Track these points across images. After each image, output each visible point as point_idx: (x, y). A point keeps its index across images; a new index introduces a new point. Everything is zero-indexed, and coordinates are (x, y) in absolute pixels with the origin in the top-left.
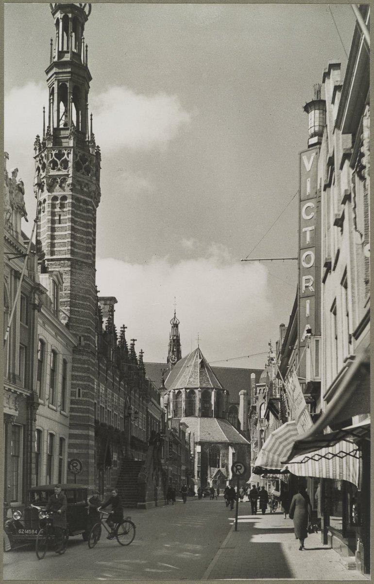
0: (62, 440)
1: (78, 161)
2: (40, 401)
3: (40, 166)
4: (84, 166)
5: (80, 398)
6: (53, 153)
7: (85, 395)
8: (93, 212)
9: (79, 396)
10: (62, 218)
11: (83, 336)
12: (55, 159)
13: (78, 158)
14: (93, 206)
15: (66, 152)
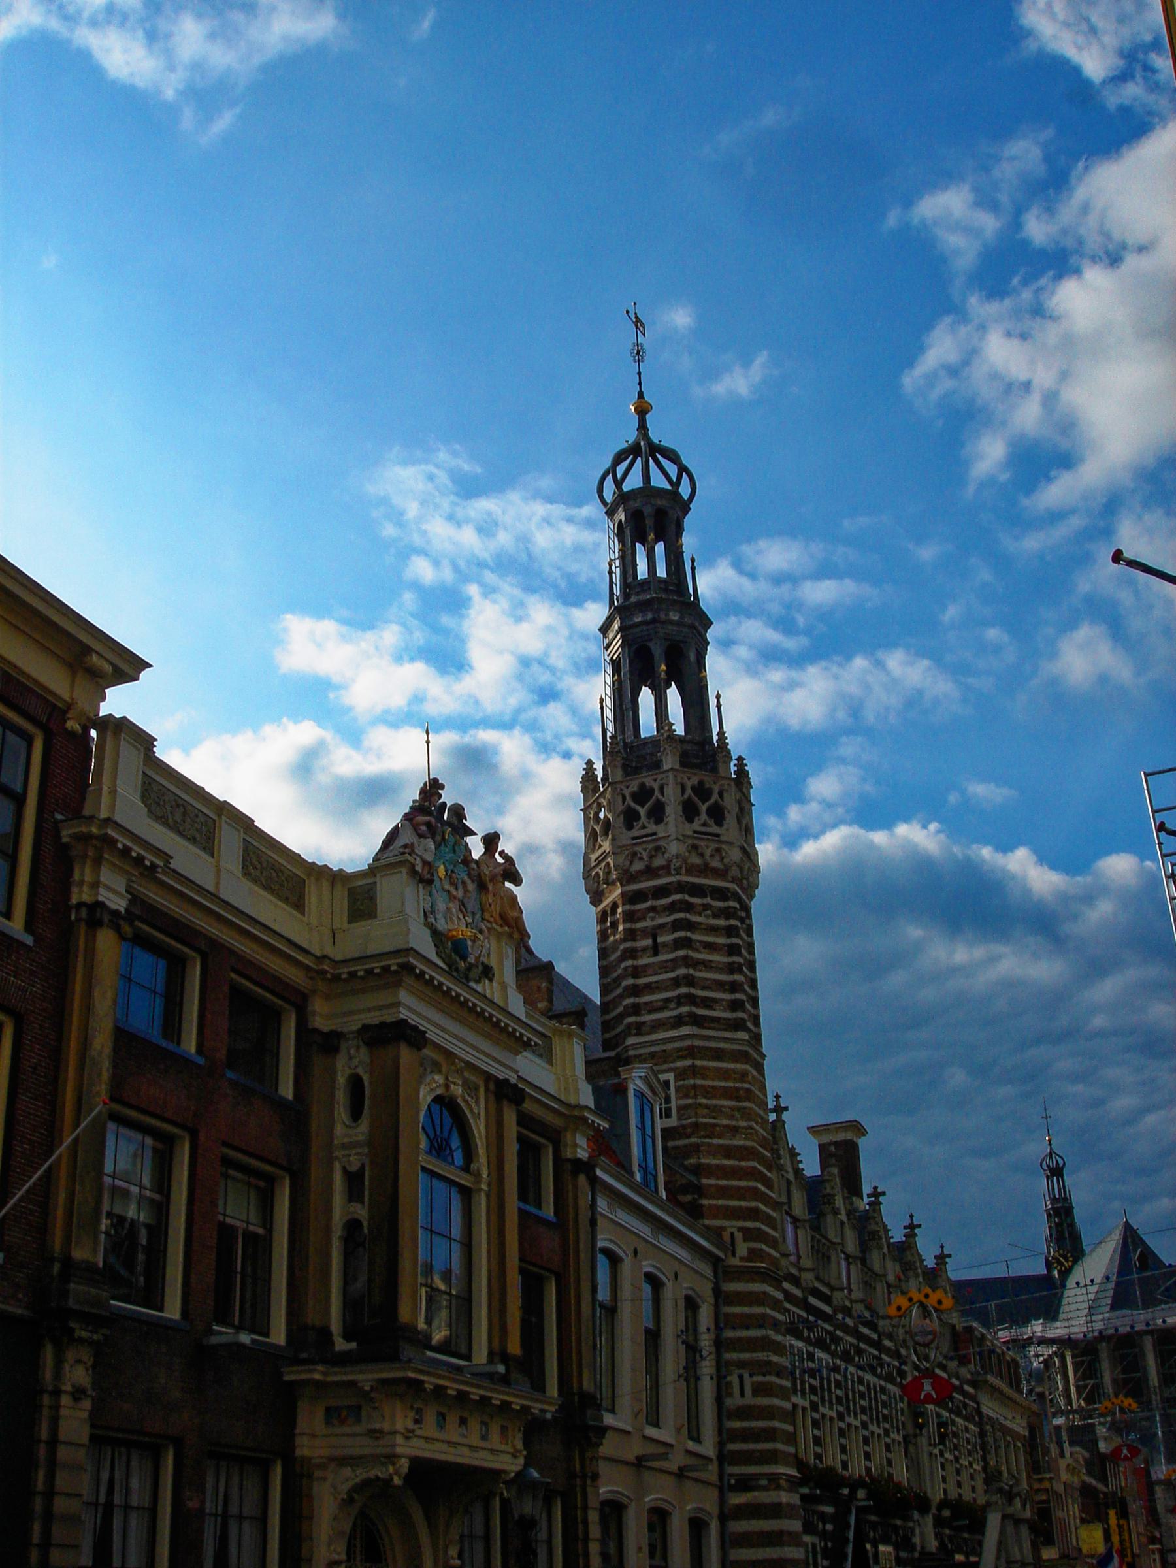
0: (697, 1526)
1: (689, 798)
2: (608, 1419)
3: (598, 828)
4: (704, 808)
5: (749, 1400)
6: (627, 793)
7: (759, 1390)
8: (743, 914)
9: (742, 1394)
10: (660, 940)
11: (740, 1229)
12: (632, 804)
13: (689, 791)
14: (739, 900)
15: (656, 786)
